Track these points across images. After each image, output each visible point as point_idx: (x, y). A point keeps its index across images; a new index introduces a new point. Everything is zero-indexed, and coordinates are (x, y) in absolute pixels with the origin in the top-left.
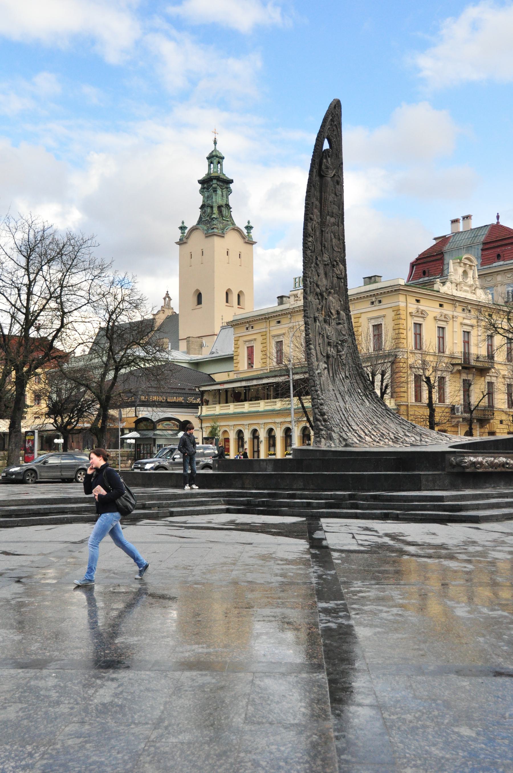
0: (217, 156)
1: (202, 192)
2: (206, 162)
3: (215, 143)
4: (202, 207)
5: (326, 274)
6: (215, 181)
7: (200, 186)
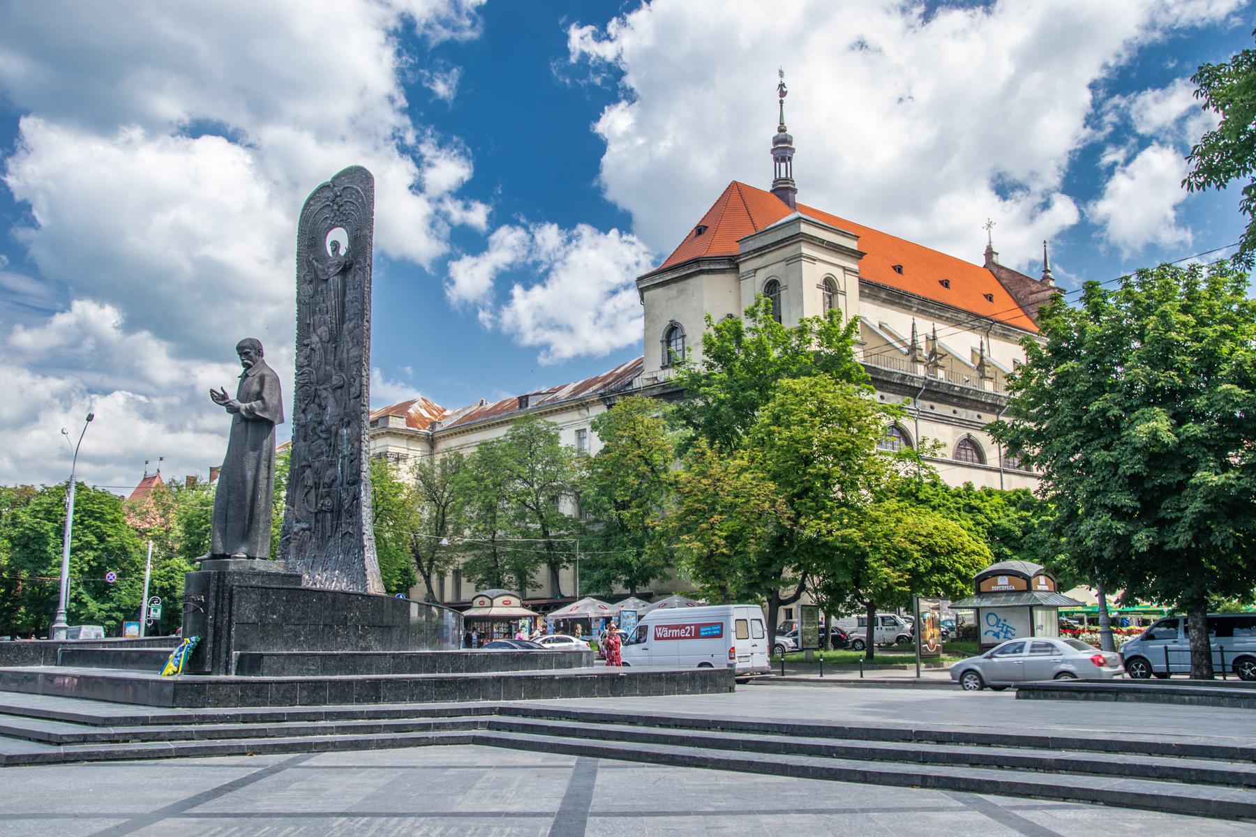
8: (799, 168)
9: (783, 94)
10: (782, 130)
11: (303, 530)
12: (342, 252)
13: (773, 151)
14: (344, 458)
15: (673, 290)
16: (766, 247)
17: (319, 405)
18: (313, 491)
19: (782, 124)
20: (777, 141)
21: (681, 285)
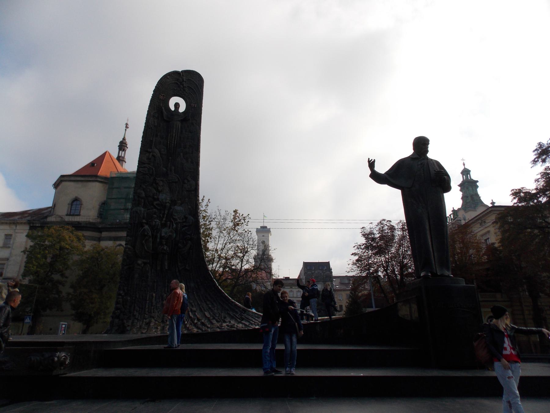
0: (466, 171)
1: (461, 190)
2: (461, 175)
3: (464, 165)
4: (462, 198)
6: (466, 184)
7: (459, 188)
9: (127, 127)
10: (124, 139)
11: (145, 263)
13: (119, 146)
14: (177, 224)
15: (79, 185)
18: (151, 239)
19: (124, 137)
21: (85, 183)
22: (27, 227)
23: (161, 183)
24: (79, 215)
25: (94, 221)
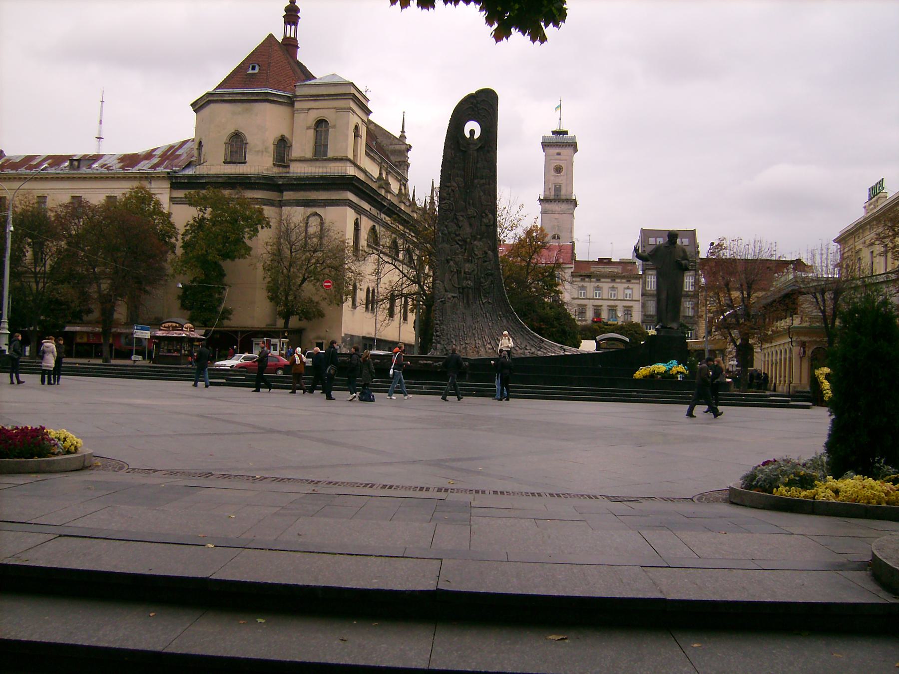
5: (471, 225)
8: (304, 32)
12: (477, 136)
15: (239, 107)
16: (322, 95)
17: (457, 225)
20: (287, 9)
22: (166, 184)
23: (461, 218)
24: (245, 163)
25: (270, 174)
